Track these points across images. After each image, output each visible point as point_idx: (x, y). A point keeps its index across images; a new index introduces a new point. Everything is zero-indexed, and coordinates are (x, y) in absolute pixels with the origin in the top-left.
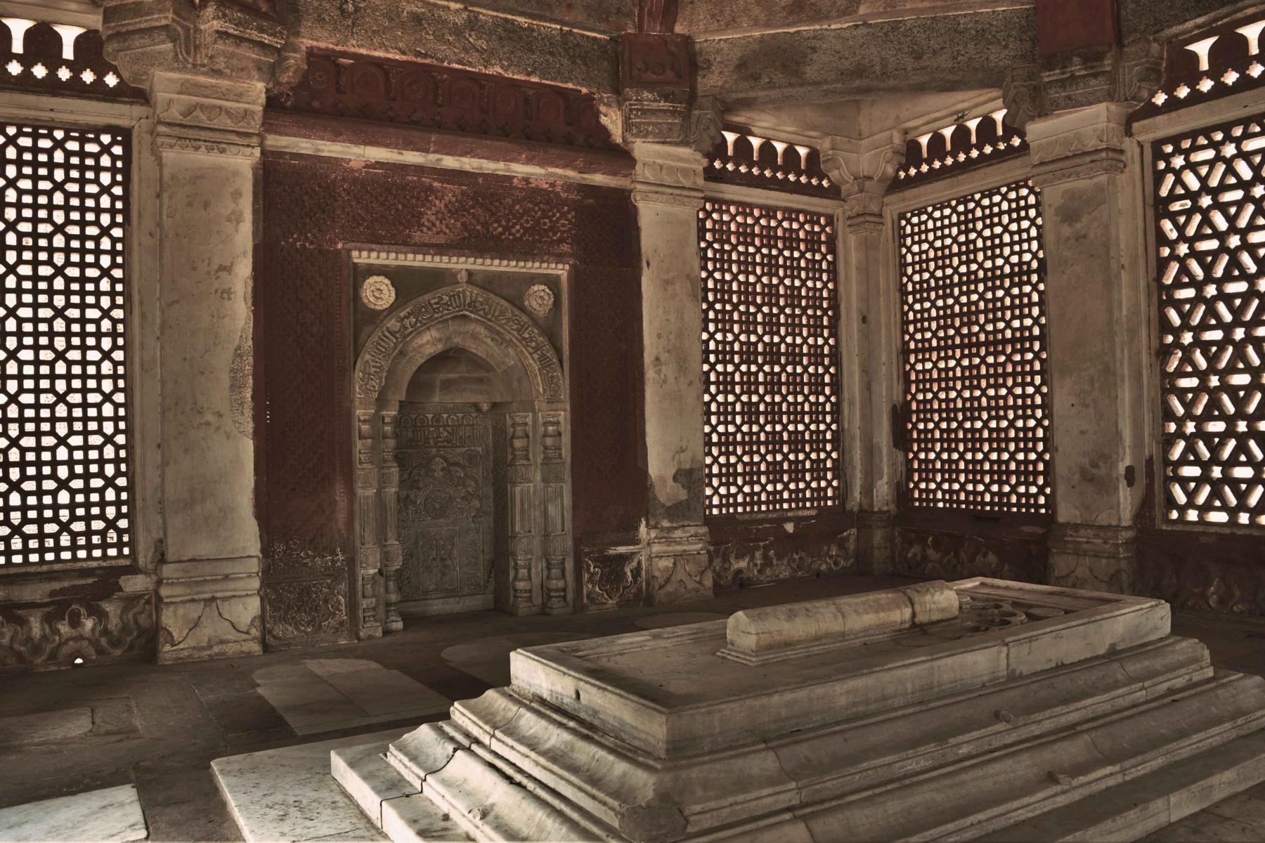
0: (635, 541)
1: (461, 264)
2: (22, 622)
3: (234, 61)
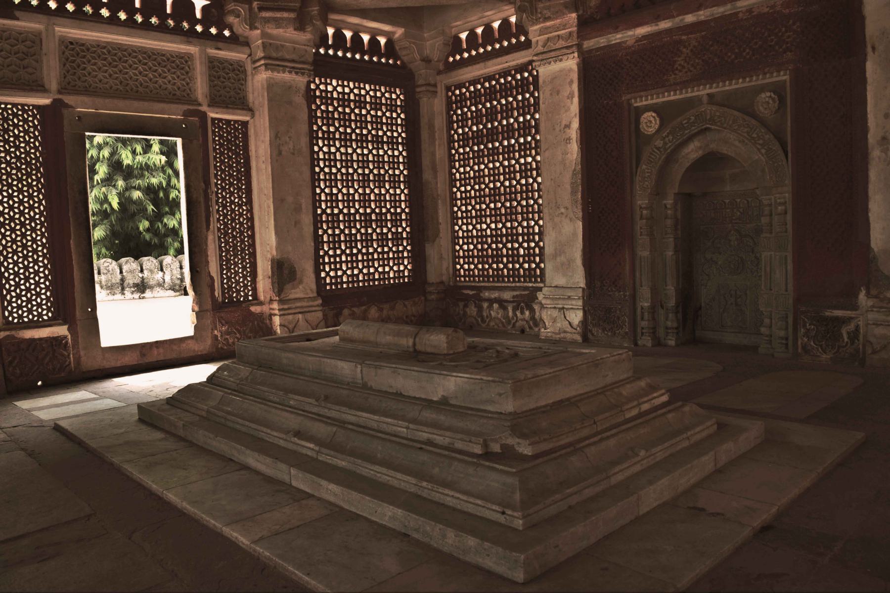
0: (855, 307)
1: (703, 92)
2: (505, 308)
3: (552, 9)
